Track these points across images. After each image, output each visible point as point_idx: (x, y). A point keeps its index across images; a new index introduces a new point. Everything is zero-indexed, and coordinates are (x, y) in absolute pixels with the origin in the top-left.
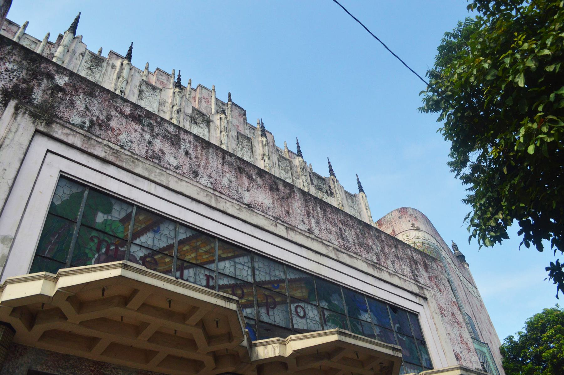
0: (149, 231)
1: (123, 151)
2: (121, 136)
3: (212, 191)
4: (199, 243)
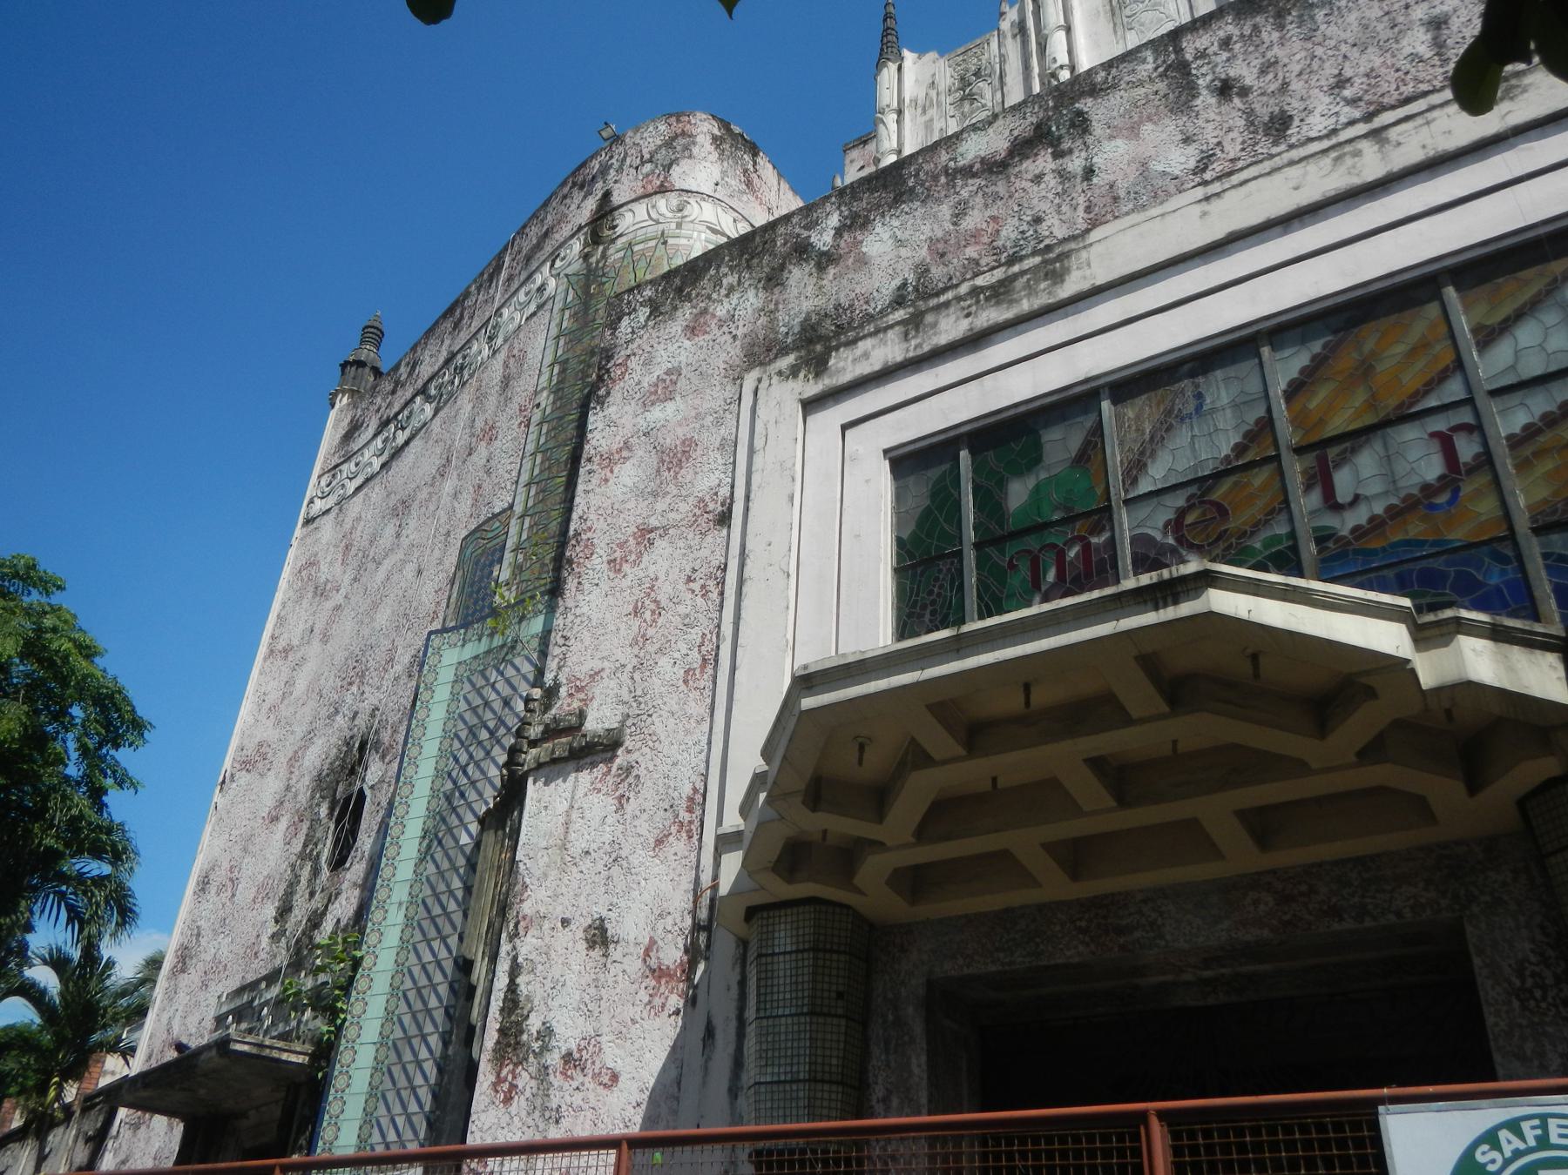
0: (1167, 430)
1: (1016, 268)
2: (1004, 233)
3: (1362, 128)
4: (1369, 345)
